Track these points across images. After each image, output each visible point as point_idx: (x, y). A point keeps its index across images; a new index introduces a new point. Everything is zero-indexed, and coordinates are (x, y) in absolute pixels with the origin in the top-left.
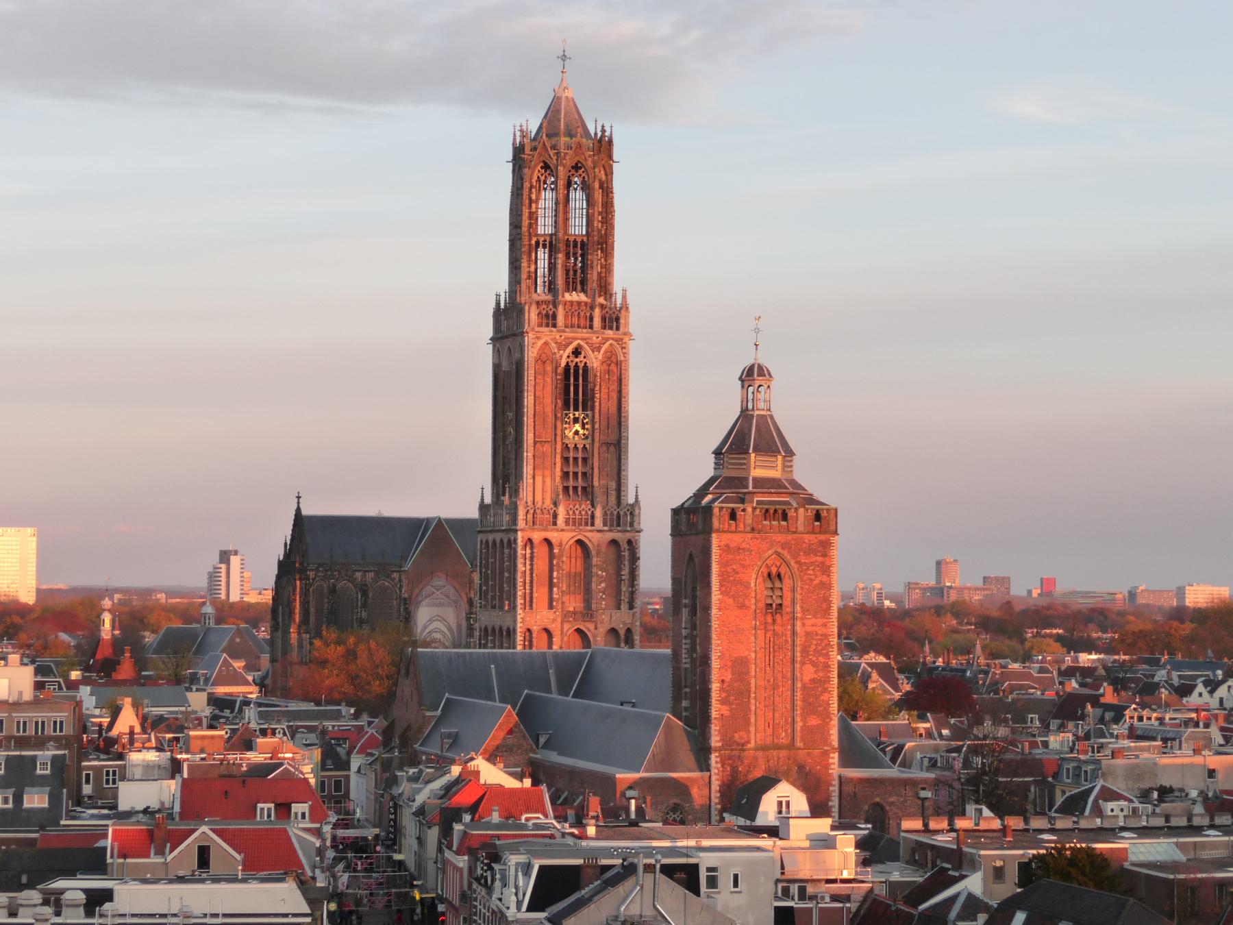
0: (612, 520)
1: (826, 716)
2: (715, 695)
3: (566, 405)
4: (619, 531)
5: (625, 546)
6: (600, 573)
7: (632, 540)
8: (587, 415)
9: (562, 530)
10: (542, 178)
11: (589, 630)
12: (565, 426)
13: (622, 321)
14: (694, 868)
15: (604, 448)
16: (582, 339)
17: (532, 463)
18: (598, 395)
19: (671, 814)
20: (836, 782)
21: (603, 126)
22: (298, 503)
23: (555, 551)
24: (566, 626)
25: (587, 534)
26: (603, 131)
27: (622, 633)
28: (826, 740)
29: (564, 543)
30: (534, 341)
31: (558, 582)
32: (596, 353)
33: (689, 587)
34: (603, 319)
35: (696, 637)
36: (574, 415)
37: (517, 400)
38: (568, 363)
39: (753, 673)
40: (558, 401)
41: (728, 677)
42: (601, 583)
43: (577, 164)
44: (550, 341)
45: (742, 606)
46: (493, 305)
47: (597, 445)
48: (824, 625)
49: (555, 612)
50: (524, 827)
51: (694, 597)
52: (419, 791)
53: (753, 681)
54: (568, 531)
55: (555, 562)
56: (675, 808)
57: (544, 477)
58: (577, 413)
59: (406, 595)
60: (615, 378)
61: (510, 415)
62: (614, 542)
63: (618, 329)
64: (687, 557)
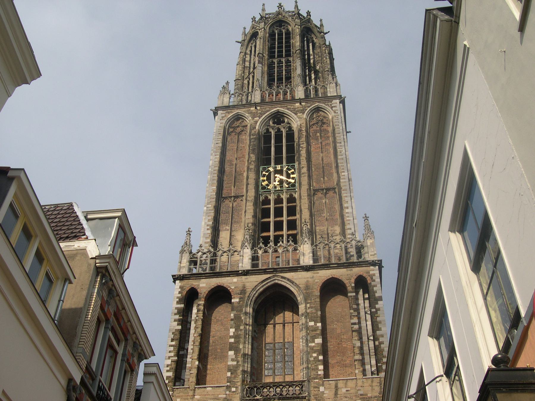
4: (340, 266)
5: (350, 285)
6: (312, 324)
8: (293, 167)
9: (246, 273)
12: (262, 178)
17: (212, 214)
23: (233, 301)
25: (288, 275)
29: (249, 291)
30: (224, 115)
31: (237, 342)
32: (299, 114)
38: (268, 130)
40: (251, 155)
58: (279, 167)
60: (330, 134)
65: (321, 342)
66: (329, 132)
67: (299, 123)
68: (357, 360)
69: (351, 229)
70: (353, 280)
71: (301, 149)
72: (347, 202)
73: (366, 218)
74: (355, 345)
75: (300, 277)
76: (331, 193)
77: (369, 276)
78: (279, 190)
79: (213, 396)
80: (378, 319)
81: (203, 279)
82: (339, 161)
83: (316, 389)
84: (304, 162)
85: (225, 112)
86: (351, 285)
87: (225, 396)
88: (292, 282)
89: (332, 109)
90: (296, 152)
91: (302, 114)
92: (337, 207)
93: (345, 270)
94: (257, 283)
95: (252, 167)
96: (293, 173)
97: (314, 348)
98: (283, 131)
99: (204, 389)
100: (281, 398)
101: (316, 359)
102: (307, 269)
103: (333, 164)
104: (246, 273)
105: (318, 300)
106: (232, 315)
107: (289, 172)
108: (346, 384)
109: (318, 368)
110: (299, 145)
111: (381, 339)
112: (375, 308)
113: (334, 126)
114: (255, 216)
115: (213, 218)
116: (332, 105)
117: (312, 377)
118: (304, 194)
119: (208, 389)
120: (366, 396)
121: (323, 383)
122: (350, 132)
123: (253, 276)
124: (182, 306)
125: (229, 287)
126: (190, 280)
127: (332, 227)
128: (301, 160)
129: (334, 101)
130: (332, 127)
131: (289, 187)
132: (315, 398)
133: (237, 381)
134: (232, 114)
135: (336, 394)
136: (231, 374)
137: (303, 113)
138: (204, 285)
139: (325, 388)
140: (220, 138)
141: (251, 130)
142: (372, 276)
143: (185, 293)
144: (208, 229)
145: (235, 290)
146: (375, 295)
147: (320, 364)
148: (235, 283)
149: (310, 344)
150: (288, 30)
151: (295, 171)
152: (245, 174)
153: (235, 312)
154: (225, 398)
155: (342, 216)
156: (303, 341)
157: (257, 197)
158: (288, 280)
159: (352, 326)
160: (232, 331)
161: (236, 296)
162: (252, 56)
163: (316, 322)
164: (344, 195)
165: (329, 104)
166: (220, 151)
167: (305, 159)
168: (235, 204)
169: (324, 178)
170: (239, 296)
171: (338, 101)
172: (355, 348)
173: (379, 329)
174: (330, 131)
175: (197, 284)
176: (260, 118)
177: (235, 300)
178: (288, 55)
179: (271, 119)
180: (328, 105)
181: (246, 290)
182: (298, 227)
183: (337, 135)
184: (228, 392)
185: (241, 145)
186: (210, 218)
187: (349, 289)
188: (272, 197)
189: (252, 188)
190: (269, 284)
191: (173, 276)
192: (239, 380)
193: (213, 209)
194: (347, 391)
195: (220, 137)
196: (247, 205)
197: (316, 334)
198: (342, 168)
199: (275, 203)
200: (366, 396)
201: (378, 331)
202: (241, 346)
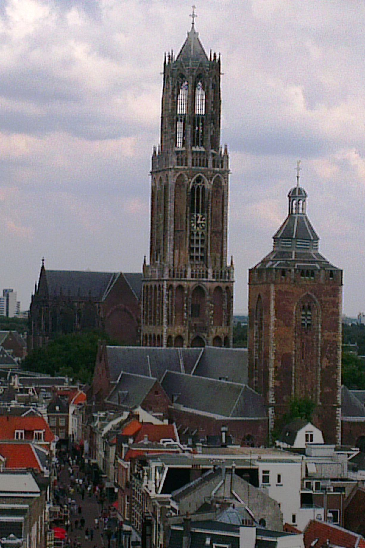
0: (217, 275)
1: (336, 387)
2: (271, 374)
3: (192, 210)
4: (221, 282)
5: (224, 290)
7: (229, 286)
10: (180, 83)
11: (204, 337)
13: (224, 163)
14: (257, 470)
16: (202, 173)
17: (173, 243)
18: (210, 205)
19: (246, 440)
20: (340, 424)
21: (215, 54)
22: (43, 263)
25: (204, 283)
26: (215, 56)
28: (335, 400)
30: (174, 174)
33: (258, 314)
34: (214, 161)
35: (262, 342)
36: (197, 215)
37: (165, 207)
39: (294, 362)
41: (279, 364)
42: (211, 310)
43: (200, 74)
44: (184, 174)
45: (288, 325)
46: (152, 153)
48: (335, 336)
49: (185, 327)
50: (162, 447)
51: (261, 319)
52: (105, 425)
53: (294, 367)
54: (193, 281)
56: (249, 437)
57: (180, 250)
59: (102, 316)
61: (161, 215)
62: (218, 288)
63: (222, 167)
64: (257, 296)
75: (209, 285)
88: (205, 287)
92: (220, 243)
104: (190, 281)
137: (211, 180)
160: (185, 305)
177: (186, 292)
188: (195, 233)
189: (188, 228)
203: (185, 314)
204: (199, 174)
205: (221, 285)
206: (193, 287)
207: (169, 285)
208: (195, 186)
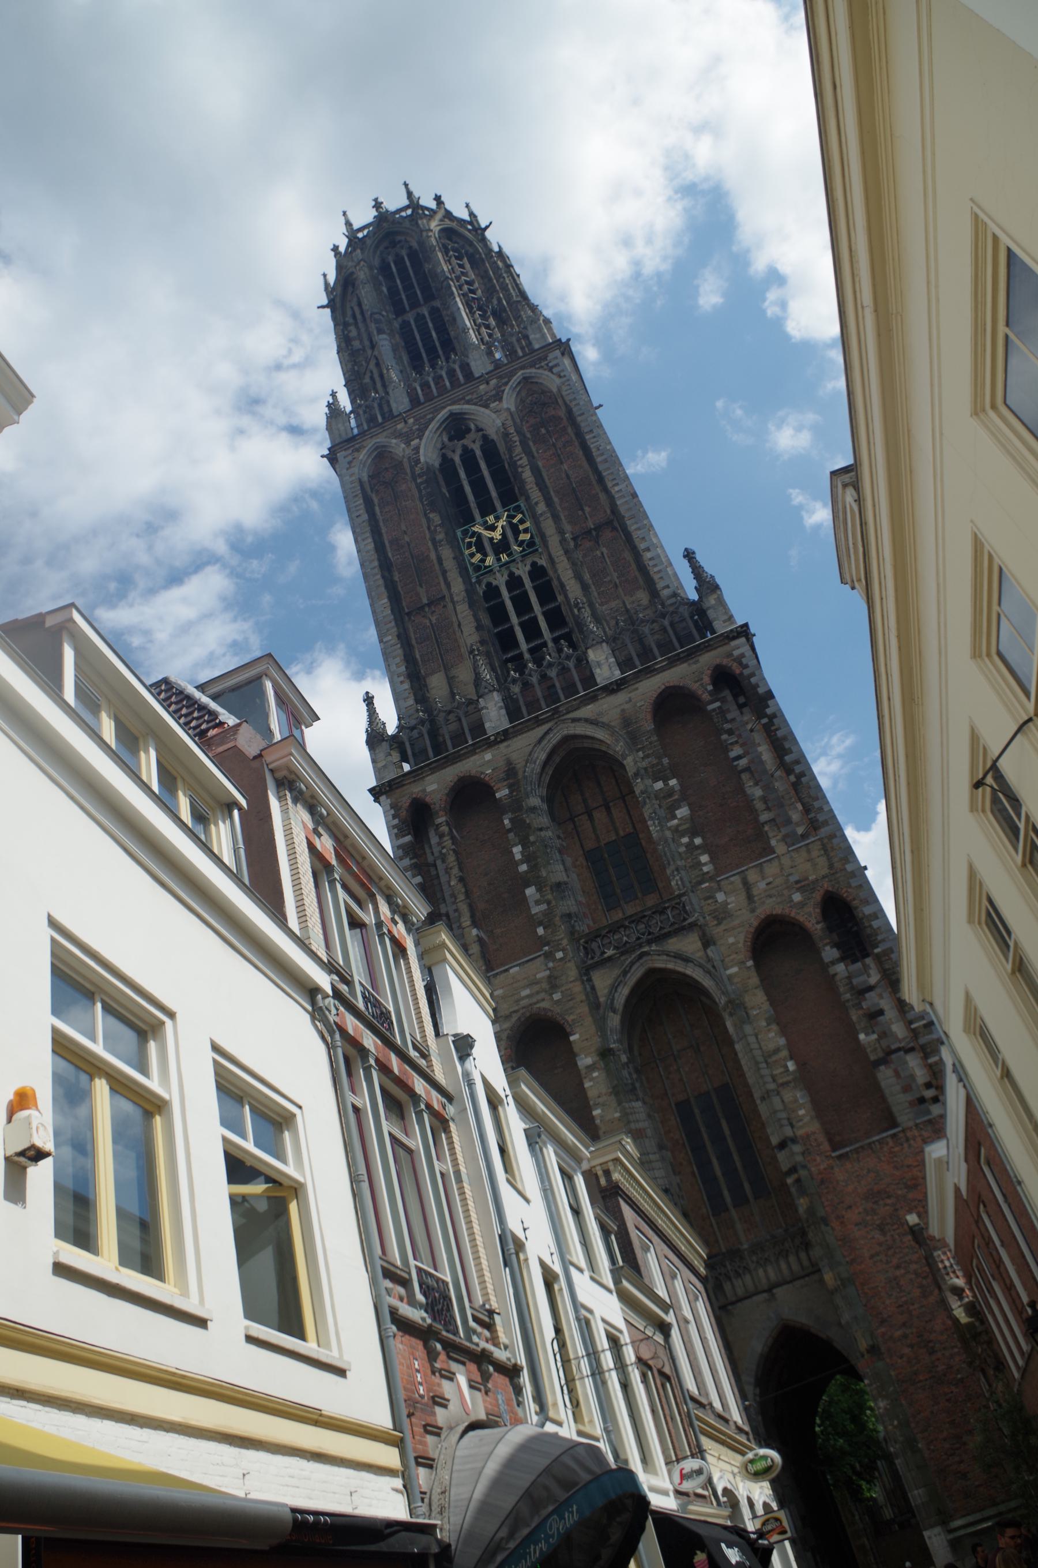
4: (673, 662)
5: (703, 688)
6: (659, 785)
7: (725, 662)
9: (505, 736)
11: (687, 960)
12: (467, 552)
15: (588, 544)
17: (400, 652)
23: (498, 795)
24: (602, 980)
27: (811, 920)
30: (350, 458)
31: (534, 868)
32: (492, 405)
38: (444, 457)
40: (431, 516)
47: (554, 542)
49: (549, 956)
55: (506, 822)
57: (447, 669)
65: (689, 812)
66: (562, 419)
67: (499, 423)
68: (766, 823)
69: (668, 587)
70: (707, 679)
71: (520, 470)
72: (644, 538)
73: (689, 555)
74: (754, 795)
76: (607, 534)
77: (734, 660)
78: (507, 563)
79: (526, 981)
80: (779, 734)
81: (428, 776)
82: (601, 467)
83: (710, 901)
84: (535, 494)
85: (350, 451)
86: (706, 689)
87: (548, 973)
89: (552, 373)
90: (512, 480)
91: (497, 403)
92: (627, 555)
93: (685, 665)
94: (531, 747)
95: (440, 536)
96: (522, 521)
97: (680, 828)
98: (475, 448)
99: (506, 974)
100: (652, 939)
101: (690, 846)
102: (614, 688)
103: (592, 477)
104: (505, 736)
105: (654, 738)
106: (506, 822)
107: (515, 521)
108: (762, 871)
109: (700, 861)
110: (513, 464)
111: (798, 769)
112: (766, 716)
113: (568, 402)
114: (479, 628)
115: (403, 658)
116: (550, 365)
117: (694, 881)
118: (557, 551)
119: (512, 971)
120: (806, 882)
121: (719, 885)
122: (601, 406)
123: (520, 737)
124: (408, 838)
125: (482, 773)
126: (405, 787)
127: (632, 596)
128: (530, 491)
129: (551, 356)
130: (563, 408)
131: (524, 550)
132: (714, 917)
133: (560, 937)
134: (365, 451)
135: (750, 897)
136: (544, 928)
137: (500, 400)
138: (434, 787)
139: (725, 893)
140: (360, 505)
141: (412, 468)
142: (739, 660)
143: (404, 813)
144: (402, 682)
145: (495, 774)
146: (757, 692)
147: (700, 854)
148: (489, 761)
149: (669, 824)
150: (411, 247)
151: (524, 515)
152: (433, 556)
153: (510, 815)
154: (549, 977)
155: (643, 569)
156: (654, 823)
157: (470, 592)
158: (586, 720)
159: (735, 763)
160: (517, 850)
161: (500, 785)
162: (361, 325)
163: (665, 780)
164: (633, 528)
165: (543, 364)
166: (368, 529)
167: (535, 486)
168: (434, 619)
169: (582, 510)
170: (505, 783)
171: (558, 353)
172: (755, 802)
173: (789, 752)
174: (563, 416)
175: (421, 788)
176: (421, 440)
177: (502, 793)
178: (429, 296)
179: (442, 432)
180: (542, 367)
181: (514, 768)
182: (567, 619)
183: (579, 419)
184: (551, 965)
185: (404, 503)
186: (398, 660)
187: (706, 697)
188: (500, 580)
190: (554, 742)
191: (371, 791)
192: (563, 936)
193: (397, 642)
194: (767, 884)
195: (358, 503)
196: (458, 611)
197: (675, 801)
198: (611, 477)
199: (510, 590)
200: (806, 882)
201: (786, 755)
202: (544, 874)
203: (530, 891)
204: (443, 414)
205: (677, 675)
206: (529, 759)
207: (405, 802)
208: (450, 455)
